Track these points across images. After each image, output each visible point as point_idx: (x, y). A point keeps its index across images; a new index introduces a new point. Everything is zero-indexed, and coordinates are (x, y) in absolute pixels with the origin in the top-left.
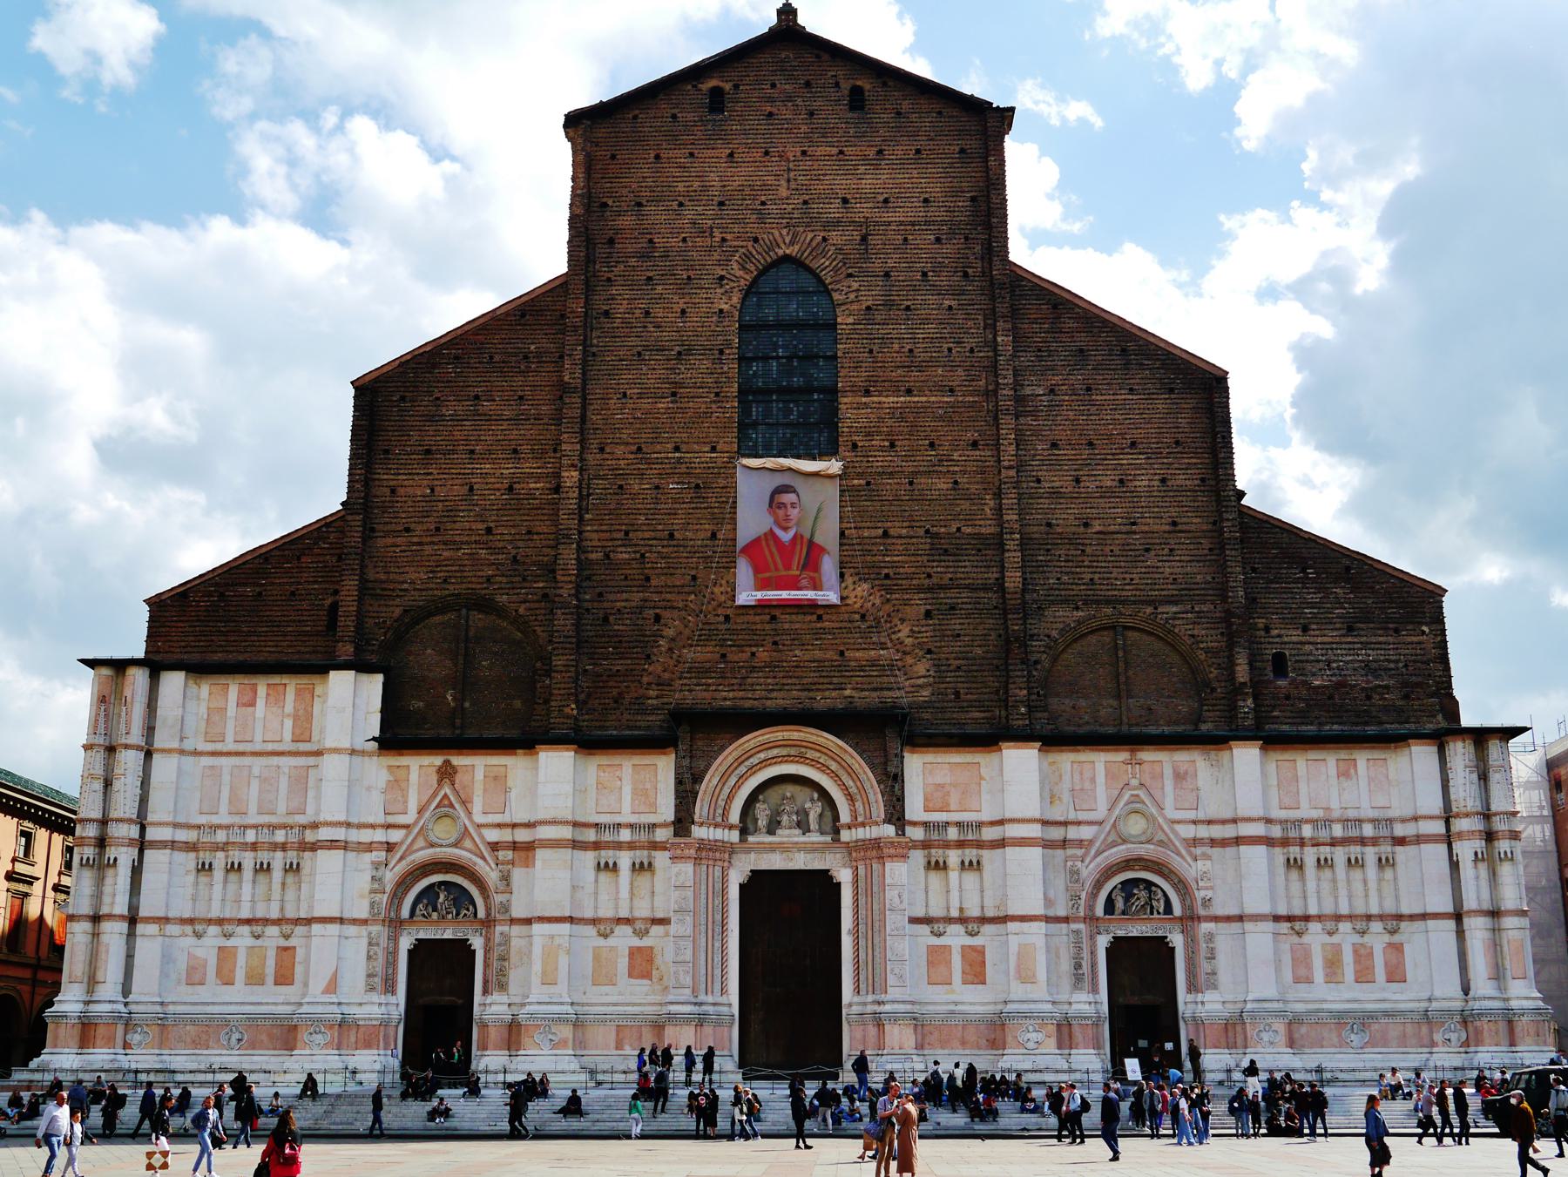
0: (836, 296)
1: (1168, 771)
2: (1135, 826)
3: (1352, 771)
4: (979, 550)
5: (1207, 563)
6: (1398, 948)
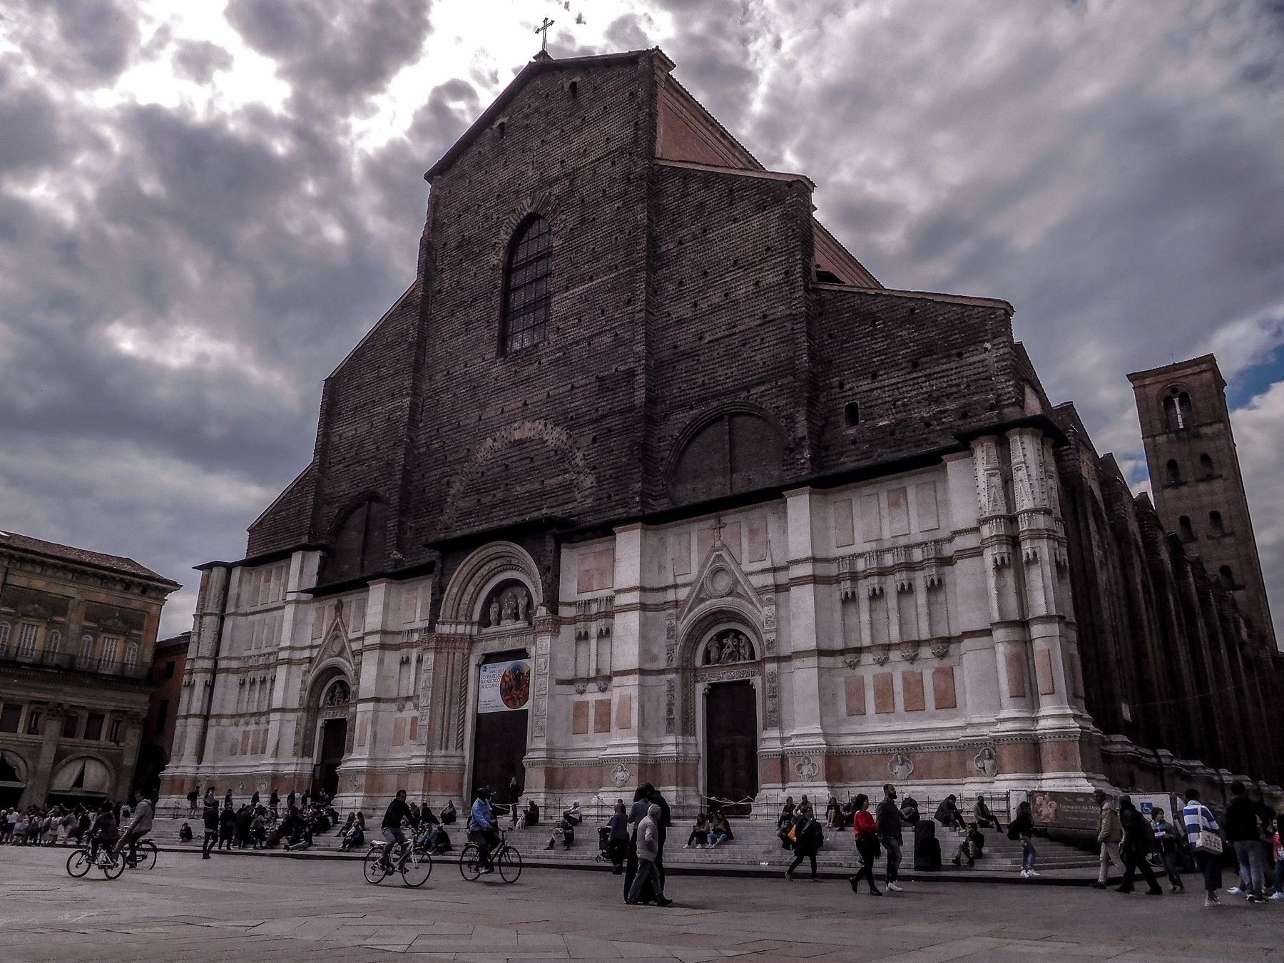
0: (554, 229)
1: (745, 531)
2: (723, 583)
3: (902, 500)
4: (629, 381)
5: (790, 342)
6: (948, 673)
